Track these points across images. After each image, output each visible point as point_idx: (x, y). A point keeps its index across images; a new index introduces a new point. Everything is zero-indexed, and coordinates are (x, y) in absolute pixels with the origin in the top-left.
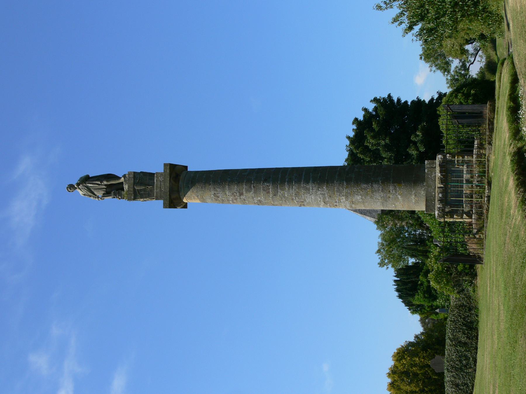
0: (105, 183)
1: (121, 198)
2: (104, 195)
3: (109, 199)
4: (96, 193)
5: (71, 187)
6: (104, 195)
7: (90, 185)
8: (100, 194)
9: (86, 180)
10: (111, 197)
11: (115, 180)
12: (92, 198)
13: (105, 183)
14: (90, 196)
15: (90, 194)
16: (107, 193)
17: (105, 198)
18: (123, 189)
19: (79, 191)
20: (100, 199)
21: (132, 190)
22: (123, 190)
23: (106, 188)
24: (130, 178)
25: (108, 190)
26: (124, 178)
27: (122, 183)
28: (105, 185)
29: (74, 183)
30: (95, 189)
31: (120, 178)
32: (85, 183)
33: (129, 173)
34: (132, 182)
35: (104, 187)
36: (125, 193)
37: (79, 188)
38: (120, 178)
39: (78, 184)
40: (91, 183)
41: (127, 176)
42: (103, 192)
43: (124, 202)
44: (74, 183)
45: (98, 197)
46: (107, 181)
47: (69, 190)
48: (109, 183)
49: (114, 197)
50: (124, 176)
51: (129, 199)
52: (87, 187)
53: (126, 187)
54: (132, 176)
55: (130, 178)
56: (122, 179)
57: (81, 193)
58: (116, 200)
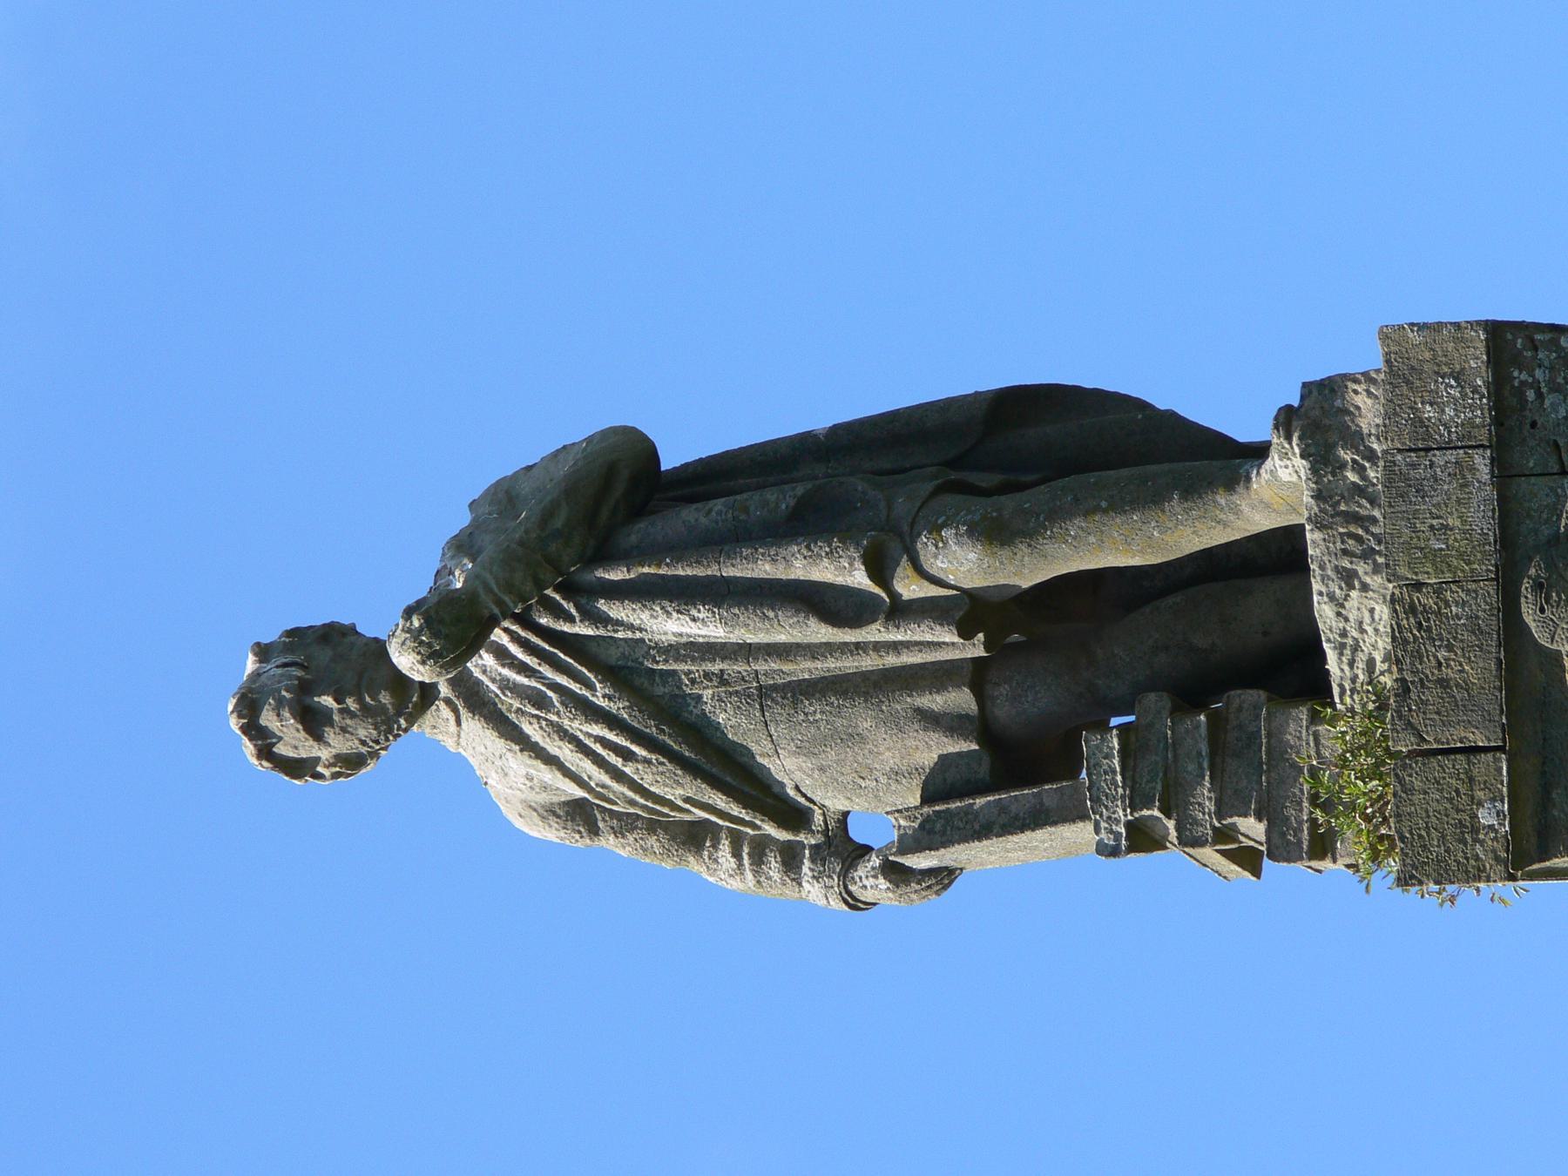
0: (959, 563)
1: (1281, 849)
2: (956, 805)
3: (1039, 867)
4: (789, 768)
5: (323, 683)
6: (956, 805)
7: (667, 625)
8: (868, 777)
9: (595, 525)
10: (1081, 834)
11: (1149, 498)
12: (722, 872)
13: (959, 563)
14: (694, 837)
15: (678, 790)
16: (1008, 772)
17: (978, 858)
18: (1297, 670)
19: (474, 741)
20: (870, 883)
21: (1476, 669)
22: (1315, 688)
23: (976, 675)
24: (1423, 444)
25: (1026, 702)
26: (1321, 459)
27: (1280, 555)
28: (969, 610)
29: (378, 598)
30: (765, 694)
31: (1230, 460)
32: (584, 594)
33: (1410, 360)
34: (1476, 514)
35: (946, 643)
36: (1335, 737)
37: (475, 700)
38: (1230, 460)
39: (453, 625)
40: (683, 594)
41: (1368, 410)
42: (930, 749)
43: (1337, 906)
44: (378, 598)
45: (841, 850)
46: (995, 535)
47: (292, 740)
48: (1026, 570)
49: (1142, 839)
50: (1317, 417)
51: (1432, 861)
52: (627, 670)
53: (1356, 624)
54: (1458, 408)
55: (1423, 444)
56: (1281, 489)
57: (509, 780)
58: (1184, 875)
